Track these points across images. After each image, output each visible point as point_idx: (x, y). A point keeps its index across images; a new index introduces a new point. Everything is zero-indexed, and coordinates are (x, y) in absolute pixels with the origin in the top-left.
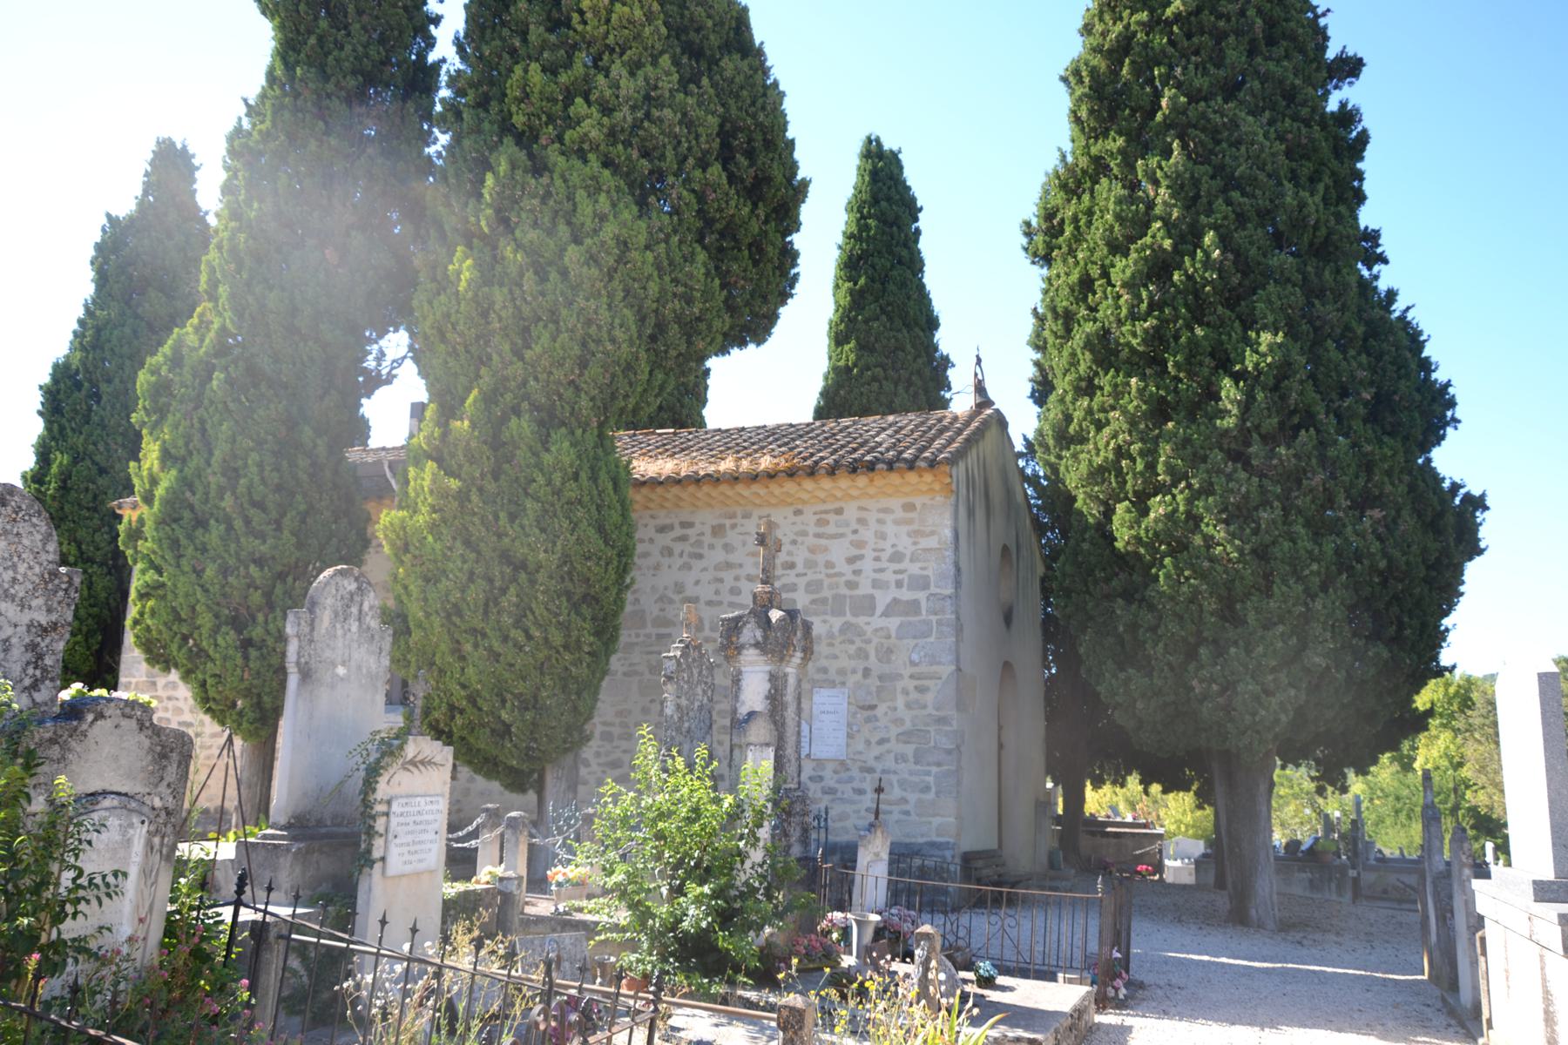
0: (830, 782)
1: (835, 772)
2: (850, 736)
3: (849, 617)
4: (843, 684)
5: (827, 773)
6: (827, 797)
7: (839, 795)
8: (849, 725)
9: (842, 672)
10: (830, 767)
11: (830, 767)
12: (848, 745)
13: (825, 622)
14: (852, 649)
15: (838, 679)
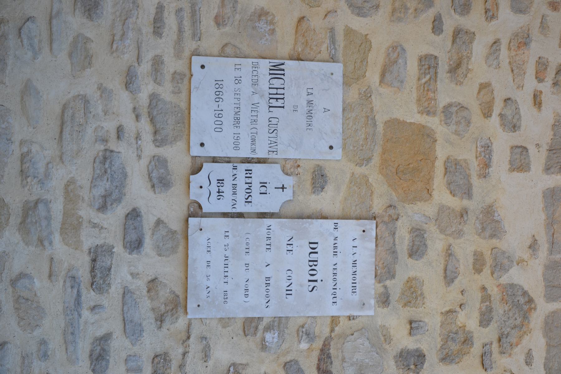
0: (126, 270)
1: (153, 284)
2: (250, 325)
3: (544, 308)
4: (384, 300)
5: (152, 262)
6: (82, 264)
7: (90, 297)
8: (278, 324)
9: (413, 293)
10: (167, 269)
11: (167, 269)
12: (225, 322)
13: (533, 246)
14: (469, 319)
15: (396, 286)
